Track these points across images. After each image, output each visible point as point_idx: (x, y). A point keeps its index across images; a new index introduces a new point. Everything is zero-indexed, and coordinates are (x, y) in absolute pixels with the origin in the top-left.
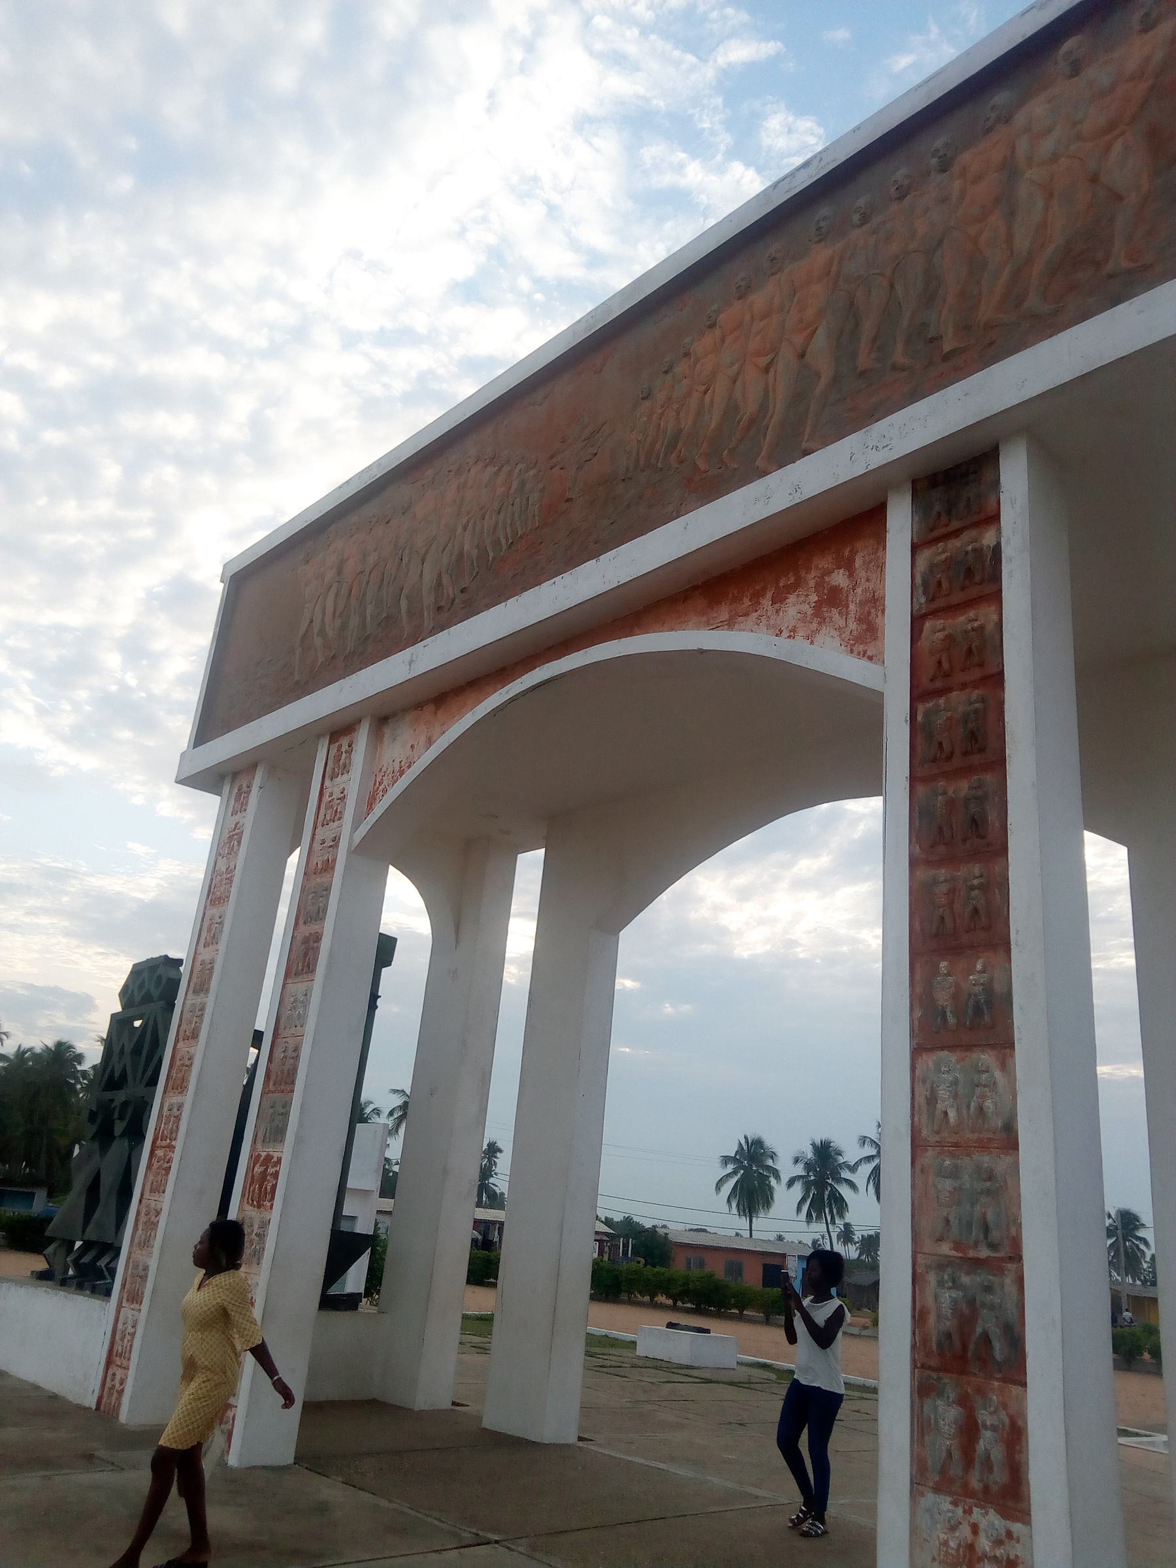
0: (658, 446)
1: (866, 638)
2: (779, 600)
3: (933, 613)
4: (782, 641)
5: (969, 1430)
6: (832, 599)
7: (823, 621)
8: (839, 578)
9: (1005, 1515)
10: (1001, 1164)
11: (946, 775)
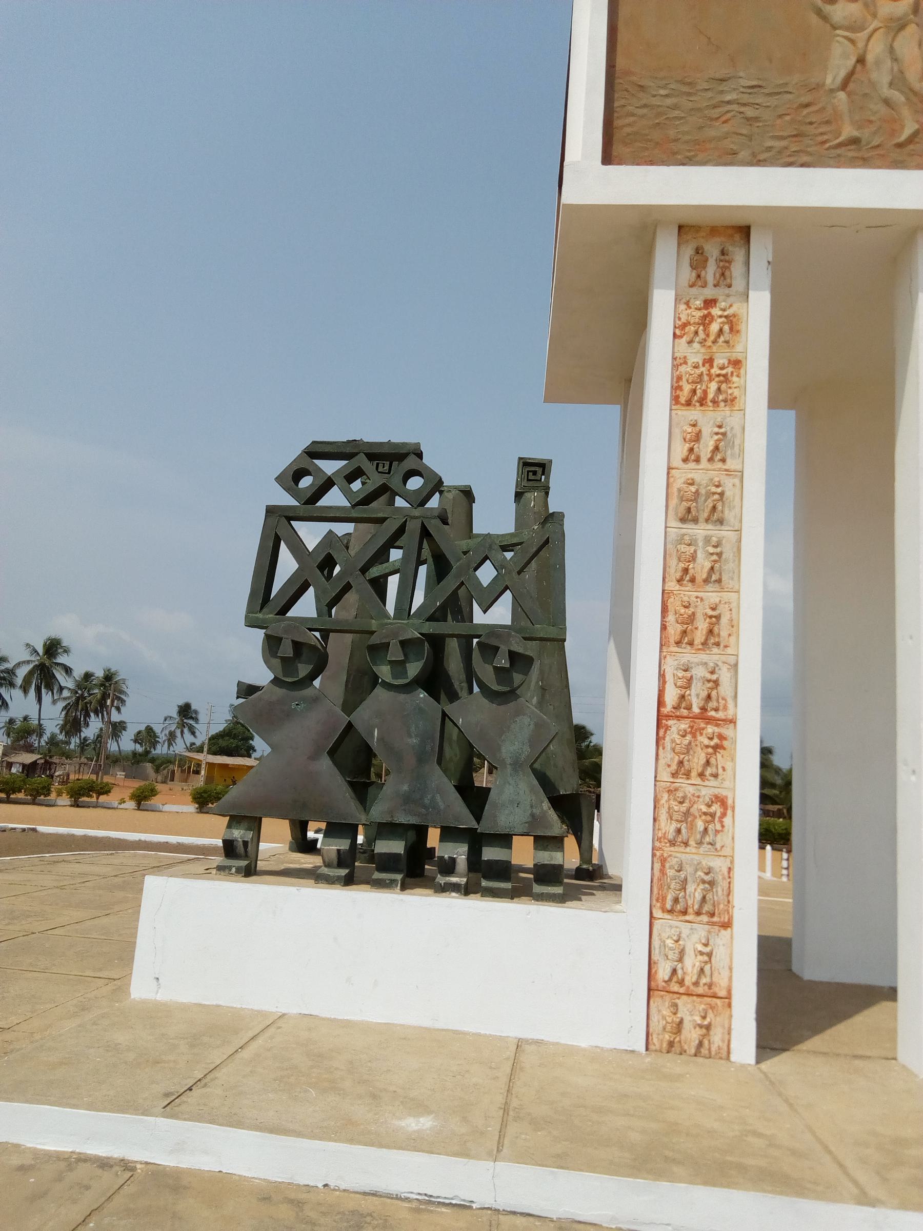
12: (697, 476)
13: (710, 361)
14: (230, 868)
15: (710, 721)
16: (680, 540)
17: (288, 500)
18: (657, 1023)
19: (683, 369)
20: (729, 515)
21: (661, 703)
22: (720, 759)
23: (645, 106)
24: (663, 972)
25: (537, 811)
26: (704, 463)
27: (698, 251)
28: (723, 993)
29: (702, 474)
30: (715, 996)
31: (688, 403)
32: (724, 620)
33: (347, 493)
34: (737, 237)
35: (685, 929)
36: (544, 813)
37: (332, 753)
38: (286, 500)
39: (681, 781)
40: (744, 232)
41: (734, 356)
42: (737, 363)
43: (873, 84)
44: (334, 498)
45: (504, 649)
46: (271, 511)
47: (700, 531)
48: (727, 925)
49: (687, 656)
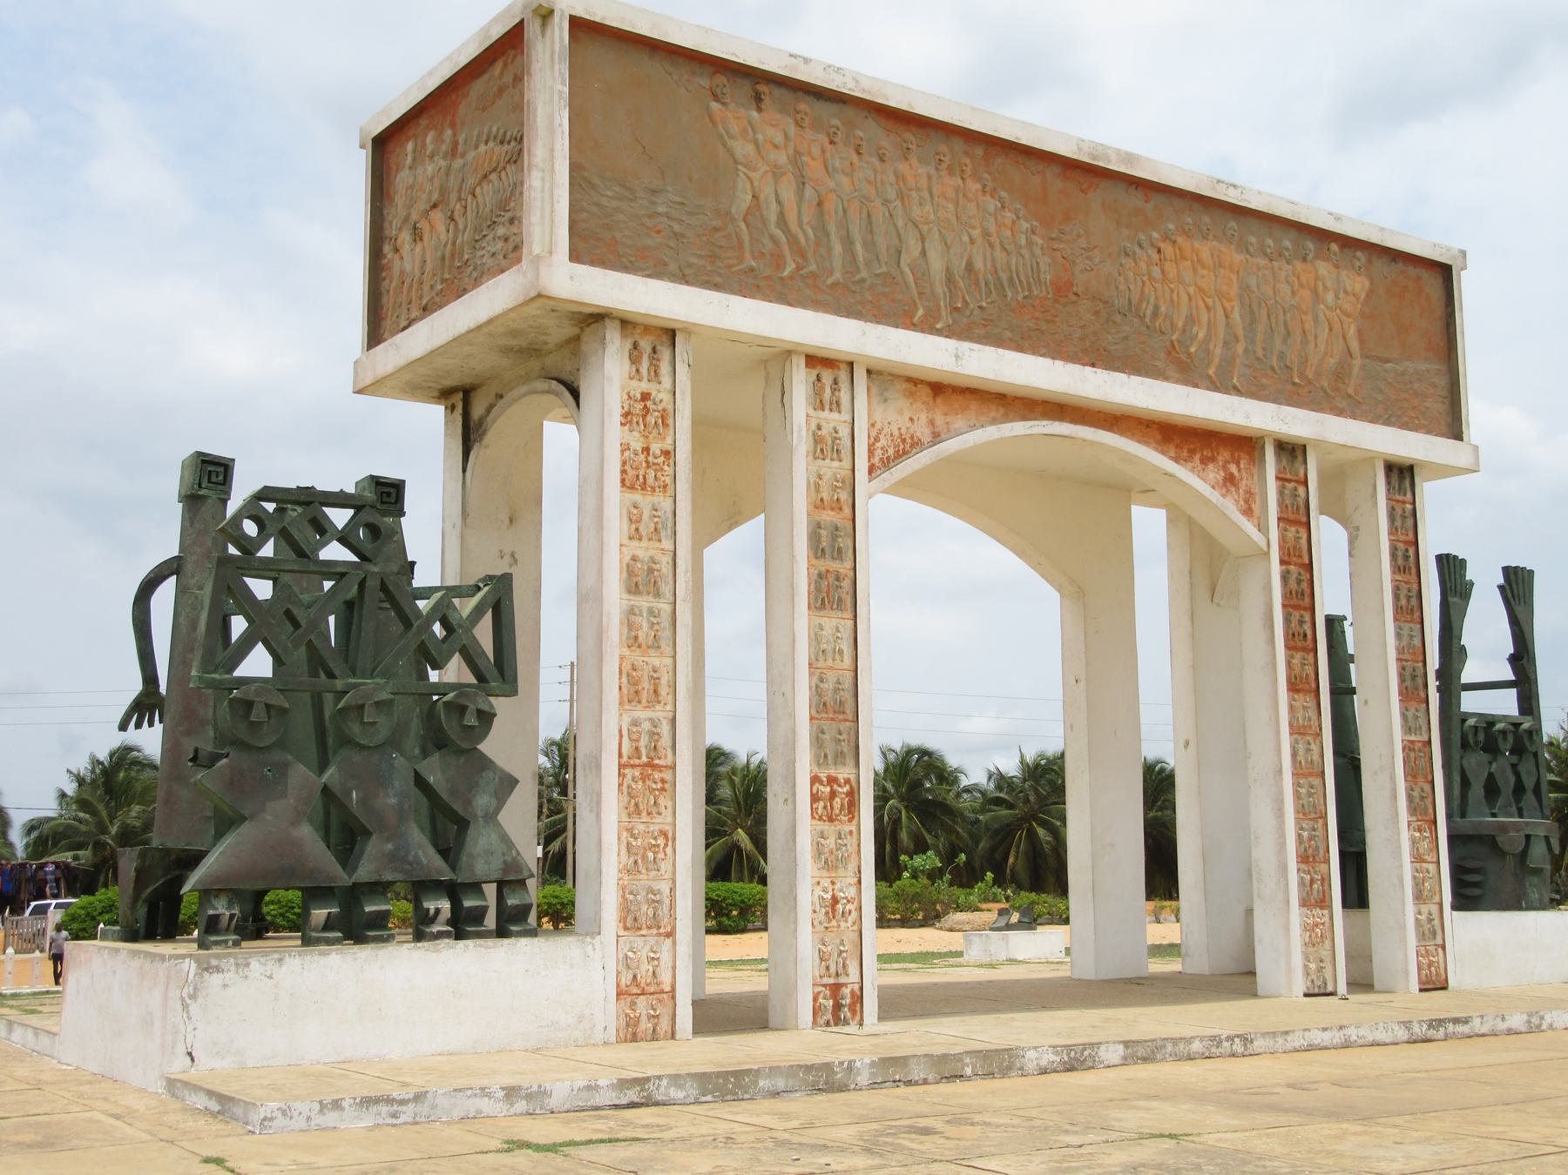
2: (1205, 461)
8: (1233, 468)
9: (1322, 908)
12: (641, 554)
13: (646, 450)
14: (226, 942)
15: (655, 767)
19: (627, 454)
23: (598, 204)
25: (509, 859)
26: (645, 540)
27: (635, 346)
28: (667, 989)
30: (662, 992)
31: (632, 488)
34: (664, 338)
35: (640, 941)
40: (670, 334)
41: (668, 445)
43: (764, 221)
45: (472, 707)
47: (644, 602)
48: (671, 934)
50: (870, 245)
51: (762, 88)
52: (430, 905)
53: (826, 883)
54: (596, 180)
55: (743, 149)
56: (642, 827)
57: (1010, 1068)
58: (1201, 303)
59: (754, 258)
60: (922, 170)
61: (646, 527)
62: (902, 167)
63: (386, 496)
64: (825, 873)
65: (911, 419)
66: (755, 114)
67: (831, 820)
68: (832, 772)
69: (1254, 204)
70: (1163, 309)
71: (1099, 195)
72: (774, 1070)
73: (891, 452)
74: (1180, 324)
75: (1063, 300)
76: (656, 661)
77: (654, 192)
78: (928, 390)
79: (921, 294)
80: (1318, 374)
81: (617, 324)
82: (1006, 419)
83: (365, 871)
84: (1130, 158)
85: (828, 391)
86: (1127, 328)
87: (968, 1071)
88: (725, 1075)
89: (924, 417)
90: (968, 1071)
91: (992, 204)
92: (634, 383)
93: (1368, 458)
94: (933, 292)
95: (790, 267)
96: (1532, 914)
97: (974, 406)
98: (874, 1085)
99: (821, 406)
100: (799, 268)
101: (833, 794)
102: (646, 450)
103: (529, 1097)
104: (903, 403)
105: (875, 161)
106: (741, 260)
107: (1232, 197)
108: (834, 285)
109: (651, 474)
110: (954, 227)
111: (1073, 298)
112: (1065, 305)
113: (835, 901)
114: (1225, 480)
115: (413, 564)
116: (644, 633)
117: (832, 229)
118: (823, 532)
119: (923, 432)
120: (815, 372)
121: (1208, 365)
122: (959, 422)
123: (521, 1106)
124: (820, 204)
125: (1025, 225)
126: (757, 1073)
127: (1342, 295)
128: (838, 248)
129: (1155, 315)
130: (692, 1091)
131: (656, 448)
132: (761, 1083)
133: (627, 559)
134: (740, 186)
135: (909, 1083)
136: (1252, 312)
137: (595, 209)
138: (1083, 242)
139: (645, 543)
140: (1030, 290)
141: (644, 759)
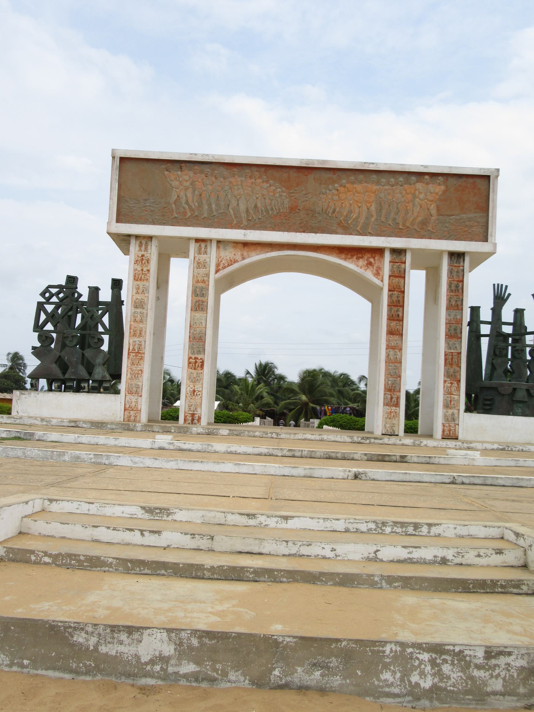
0: (329, 209)
1: (378, 273)
2: (358, 258)
3: (393, 276)
4: (358, 268)
5: (392, 398)
6: (370, 264)
7: (368, 268)
8: (372, 260)
9: (396, 407)
10: (399, 365)
11: (393, 306)
12: (139, 297)
13: (142, 270)
16: (135, 313)
17: (43, 300)
18: (126, 416)
20: (145, 307)
21: (129, 350)
22: (141, 362)
24: (127, 406)
27: (141, 243)
29: (139, 297)
31: (137, 280)
32: (144, 331)
33: (58, 298)
35: (132, 397)
36: (105, 375)
37: (56, 363)
38: (43, 300)
39: (133, 366)
41: (148, 269)
42: (148, 271)
43: (181, 203)
44: (54, 299)
45: (96, 337)
46: (39, 303)
47: (139, 310)
48: (141, 396)
49: (136, 339)
50: (218, 205)
51: (181, 165)
52: (82, 385)
53: (192, 386)
54: (128, 200)
55: (175, 183)
56: (134, 368)
57: (187, 431)
58: (356, 206)
59: (177, 214)
60: (239, 179)
61: (140, 291)
62: (232, 180)
63: (117, 284)
64: (192, 383)
65: (235, 254)
66: (179, 173)
67: (195, 369)
68: (196, 356)
69: (382, 169)
70: (337, 210)
71: (311, 176)
72: (112, 423)
73: (226, 265)
74: (345, 214)
75: (293, 212)
76: (141, 326)
77: (146, 200)
78: (242, 245)
79: (236, 217)
80: (413, 224)
81: (134, 237)
82: (272, 251)
83: (67, 376)
84: (324, 162)
85: (203, 249)
86: (320, 218)
87: (173, 431)
88: (98, 423)
89: (239, 253)
90: (173, 431)
91: (265, 185)
92: (140, 252)
93: (440, 253)
94: (240, 216)
95: (189, 214)
96: (516, 417)
97: (259, 248)
98: (141, 431)
99: (200, 253)
100: (192, 215)
101: (196, 362)
102: (142, 270)
103: (47, 421)
104: (232, 250)
105: (222, 179)
106: (172, 215)
107: (372, 167)
108: (204, 218)
109: (143, 276)
110: (246, 194)
111: (298, 211)
112: (294, 214)
113: (194, 391)
114: (367, 264)
115: (123, 301)
116: (138, 319)
117: (204, 202)
118: (198, 289)
119: (238, 257)
120: (198, 244)
121: (358, 226)
122: (253, 253)
123: (45, 423)
124: (200, 195)
125: (279, 190)
126: (107, 424)
127: (428, 194)
128: (206, 207)
129: (334, 212)
130: (88, 425)
131: (145, 269)
132: (108, 426)
133: (134, 299)
134: (173, 194)
135: (153, 431)
136: (381, 206)
137: (127, 207)
138: (304, 193)
139: (140, 295)
140: (279, 210)
141: (136, 351)
